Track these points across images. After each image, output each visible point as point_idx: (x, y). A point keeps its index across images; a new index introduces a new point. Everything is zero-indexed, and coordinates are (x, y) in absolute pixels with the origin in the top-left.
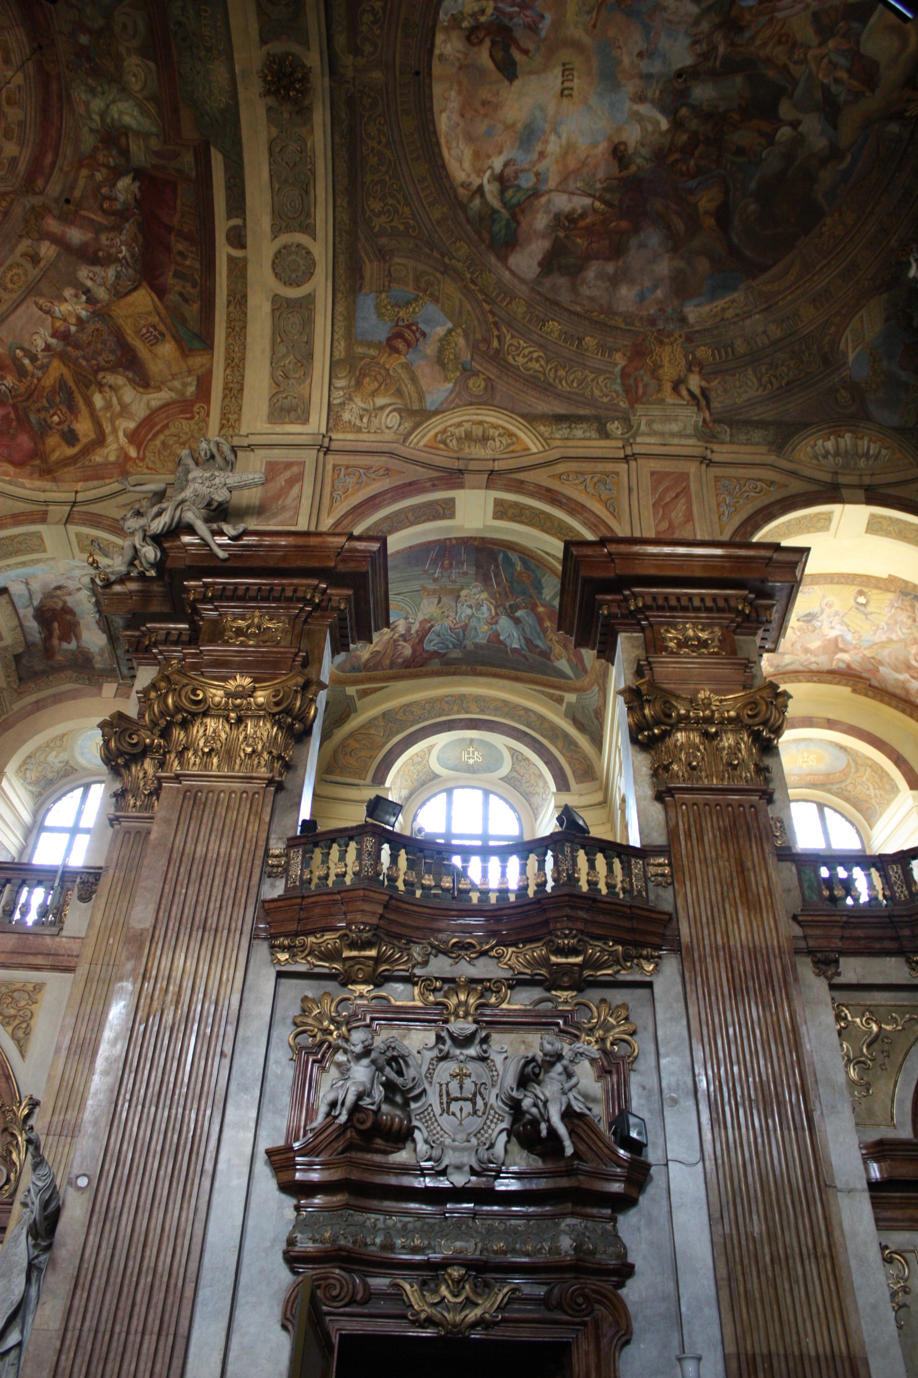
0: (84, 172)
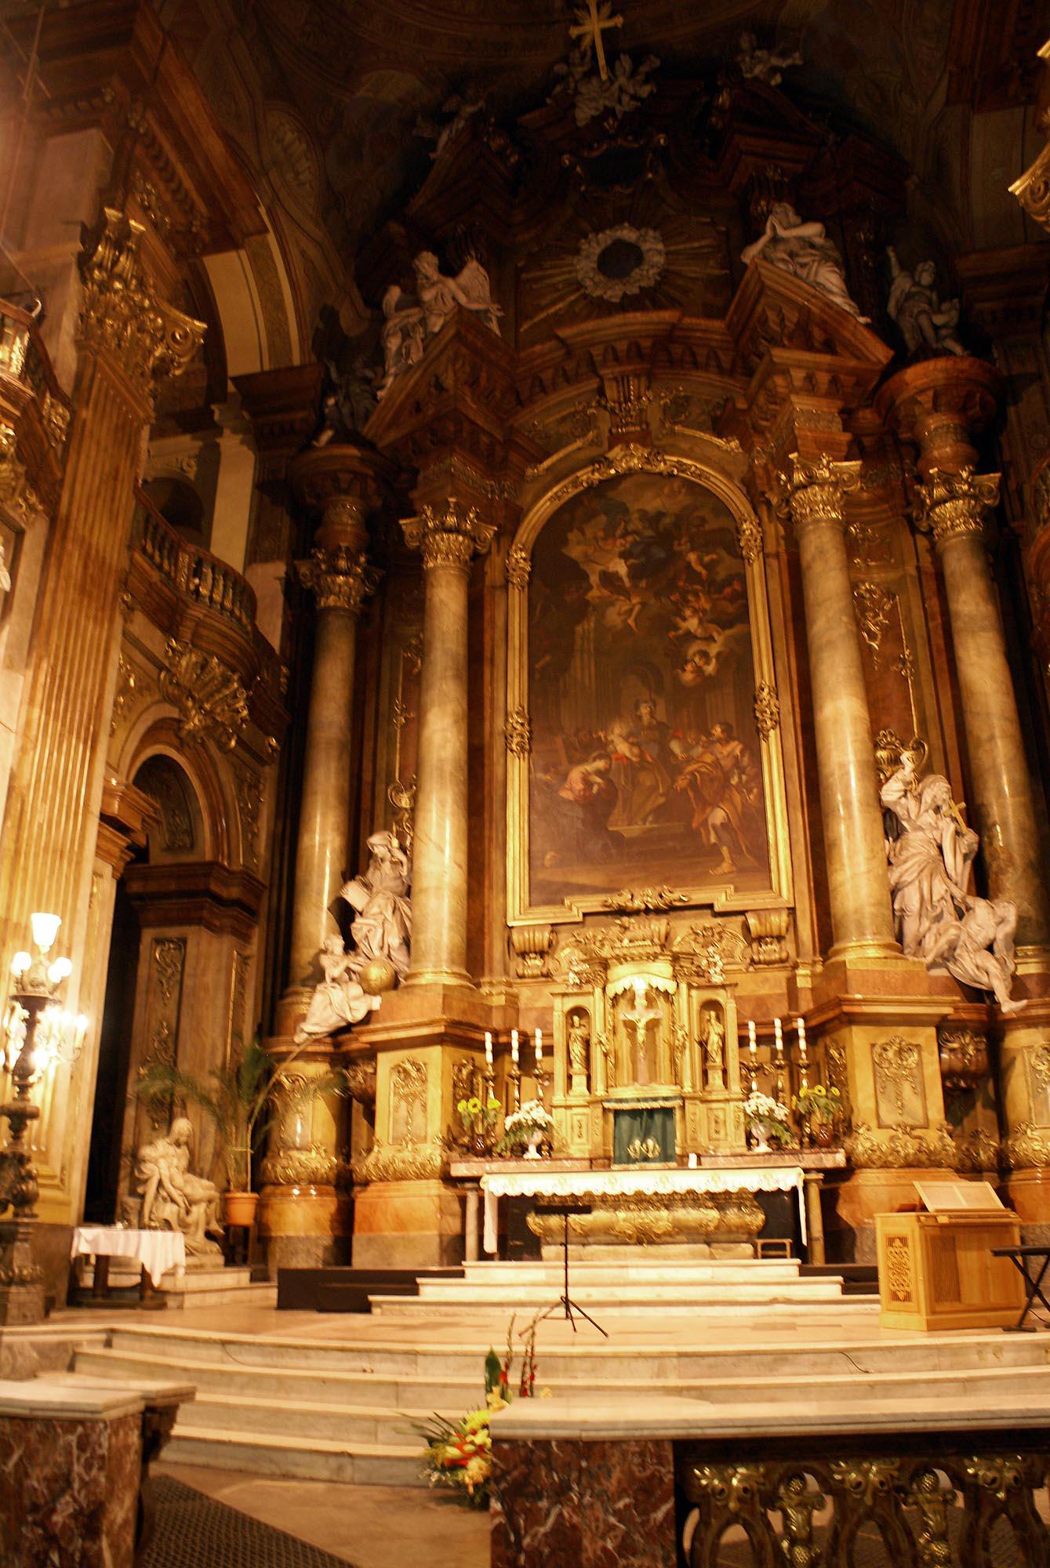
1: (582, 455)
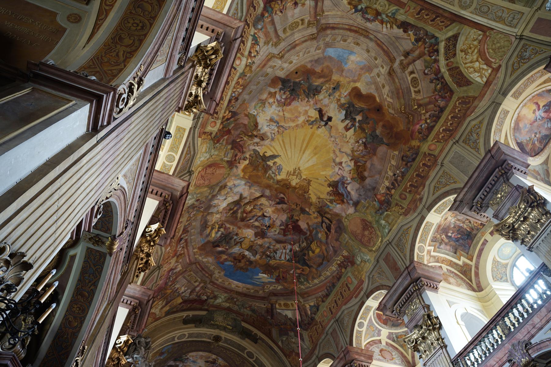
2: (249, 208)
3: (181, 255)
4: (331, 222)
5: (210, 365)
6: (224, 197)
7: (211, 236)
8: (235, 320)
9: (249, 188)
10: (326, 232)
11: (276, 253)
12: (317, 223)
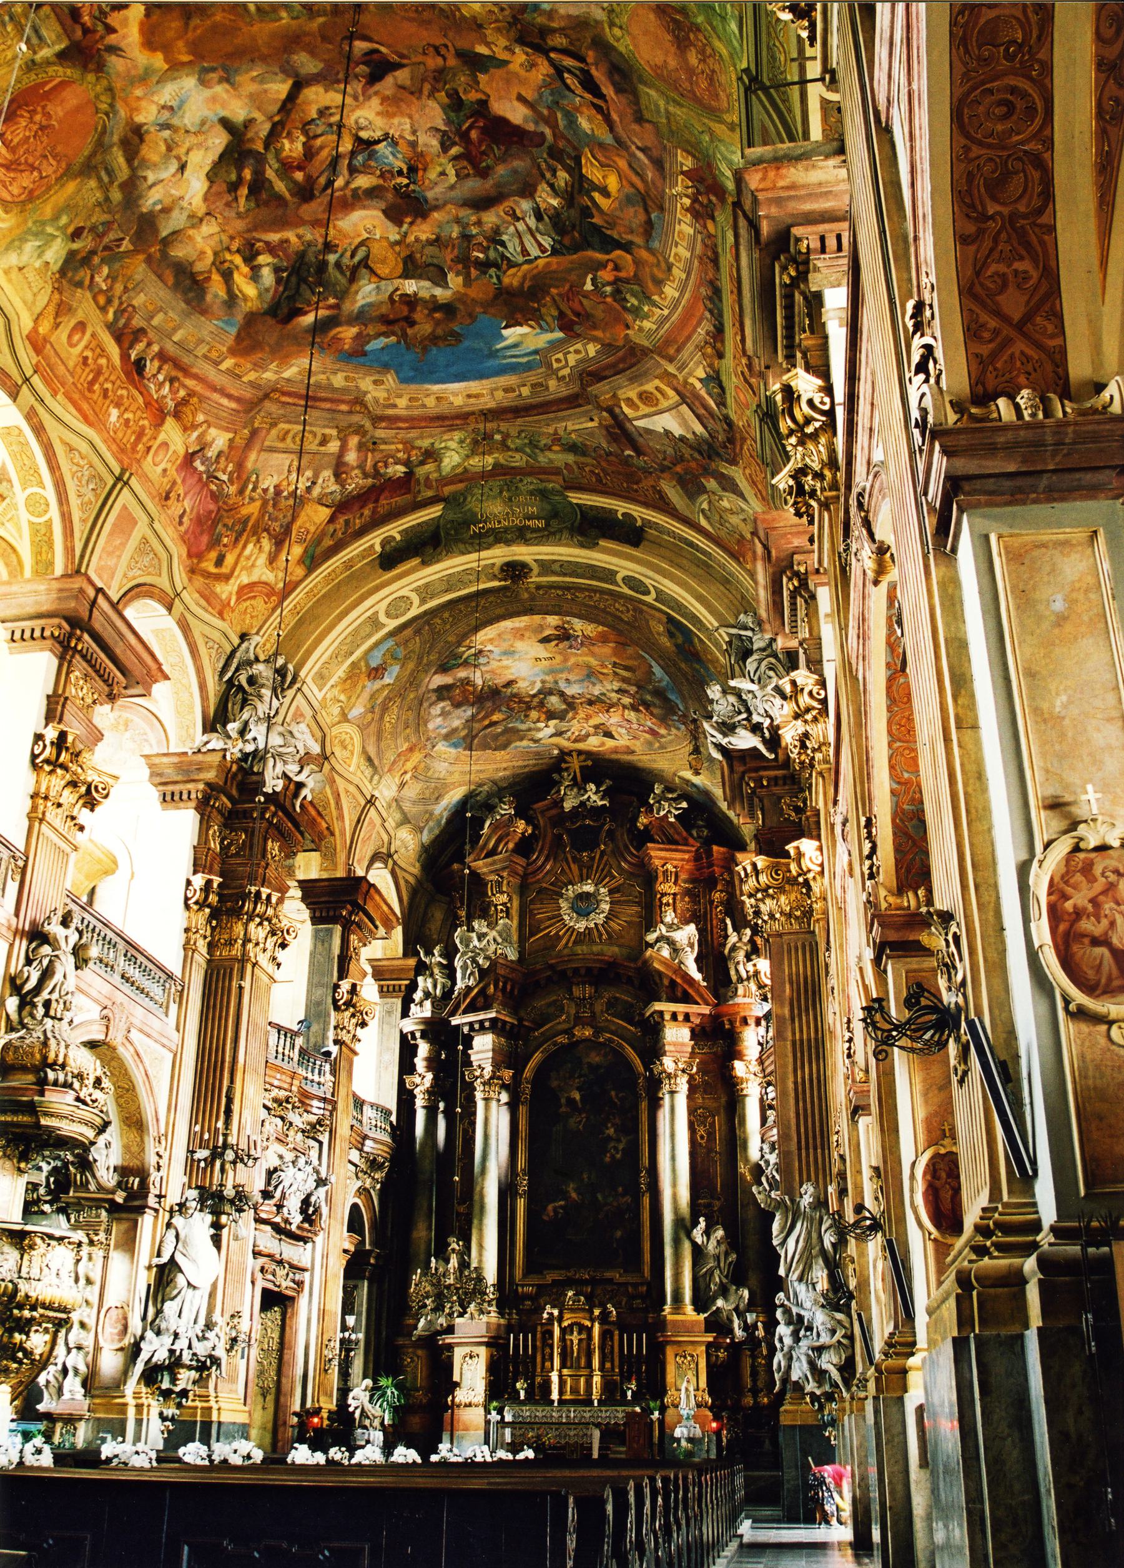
0: (400, 446)
1: (560, 1027)
2: (293, 147)
3: (184, 402)
4: (582, 59)
5: (561, 646)
6: (174, 166)
7: (246, 298)
8: (543, 494)
9: (227, 86)
10: (593, 104)
11: (503, 244)
12: (545, 85)
